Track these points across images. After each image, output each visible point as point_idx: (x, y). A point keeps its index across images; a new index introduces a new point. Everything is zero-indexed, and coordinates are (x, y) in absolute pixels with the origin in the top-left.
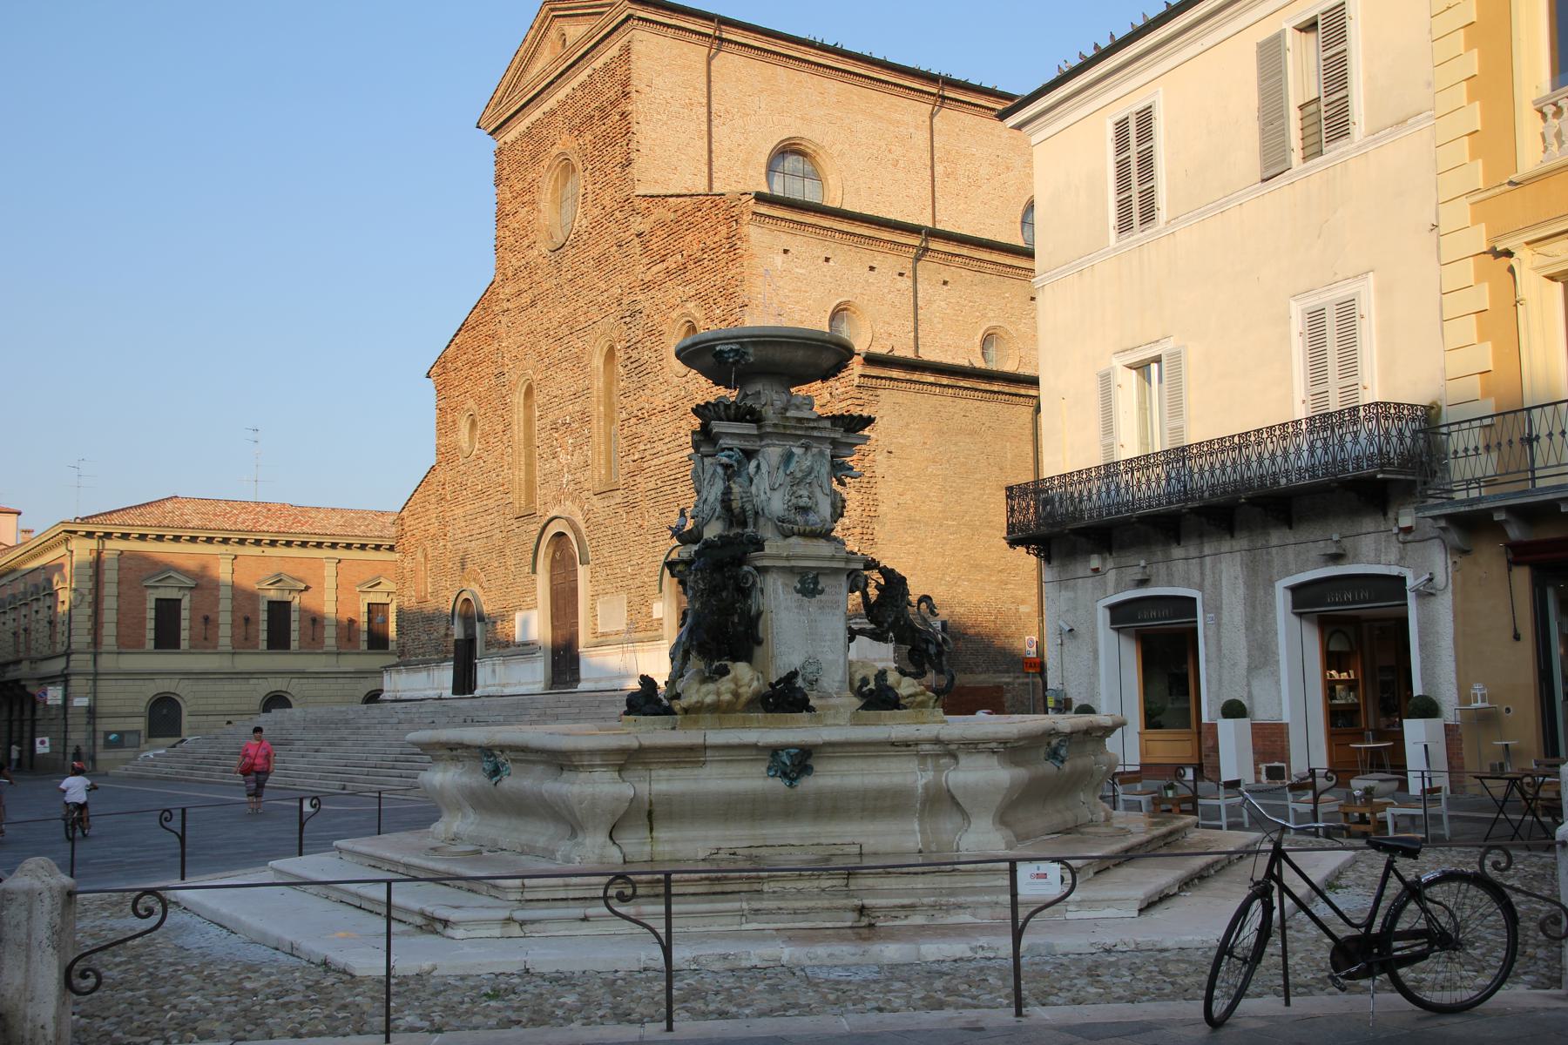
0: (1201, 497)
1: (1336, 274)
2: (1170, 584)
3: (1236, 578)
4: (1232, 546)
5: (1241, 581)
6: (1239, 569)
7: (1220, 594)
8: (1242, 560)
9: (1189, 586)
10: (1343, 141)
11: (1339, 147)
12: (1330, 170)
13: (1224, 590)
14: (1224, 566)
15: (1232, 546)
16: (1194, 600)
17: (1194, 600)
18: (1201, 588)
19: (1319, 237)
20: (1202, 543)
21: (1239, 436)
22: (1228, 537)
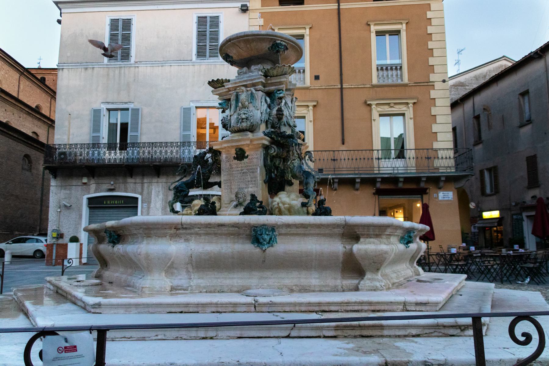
0: (159, 162)
1: (209, 98)
2: (126, 192)
3: (159, 192)
4: (158, 181)
5: (161, 193)
6: (161, 189)
7: (151, 197)
8: (162, 186)
9: (135, 193)
10: (216, 58)
11: (214, 59)
12: (209, 65)
13: (153, 196)
14: (153, 187)
15: (158, 181)
16: (137, 198)
17: (137, 198)
18: (141, 194)
19: (204, 85)
20: (143, 178)
21: (180, 142)
22: (157, 177)
